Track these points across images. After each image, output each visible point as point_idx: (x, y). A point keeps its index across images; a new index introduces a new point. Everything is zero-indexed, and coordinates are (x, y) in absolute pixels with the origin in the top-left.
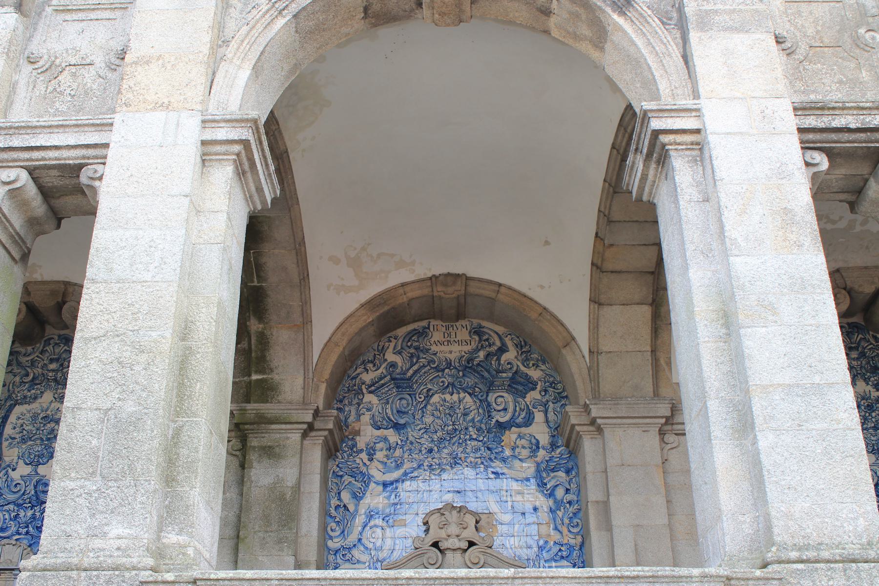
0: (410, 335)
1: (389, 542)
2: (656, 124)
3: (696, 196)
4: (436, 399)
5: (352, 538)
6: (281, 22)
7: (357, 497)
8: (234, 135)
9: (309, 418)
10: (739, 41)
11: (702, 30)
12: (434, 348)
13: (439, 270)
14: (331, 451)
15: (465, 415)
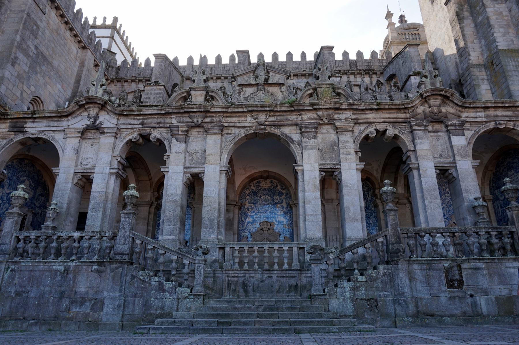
0: (256, 183)
1: (252, 228)
2: (296, 168)
3: (302, 181)
4: (262, 197)
5: (245, 227)
6: (232, 145)
7: (245, 219)
8: (225, 169)
9: (235, 203)
10: (311, 152)
11: (305, 149)
12: (262, 186)
13: (262, 170)
14: (240, 209)
15: (268, 201)
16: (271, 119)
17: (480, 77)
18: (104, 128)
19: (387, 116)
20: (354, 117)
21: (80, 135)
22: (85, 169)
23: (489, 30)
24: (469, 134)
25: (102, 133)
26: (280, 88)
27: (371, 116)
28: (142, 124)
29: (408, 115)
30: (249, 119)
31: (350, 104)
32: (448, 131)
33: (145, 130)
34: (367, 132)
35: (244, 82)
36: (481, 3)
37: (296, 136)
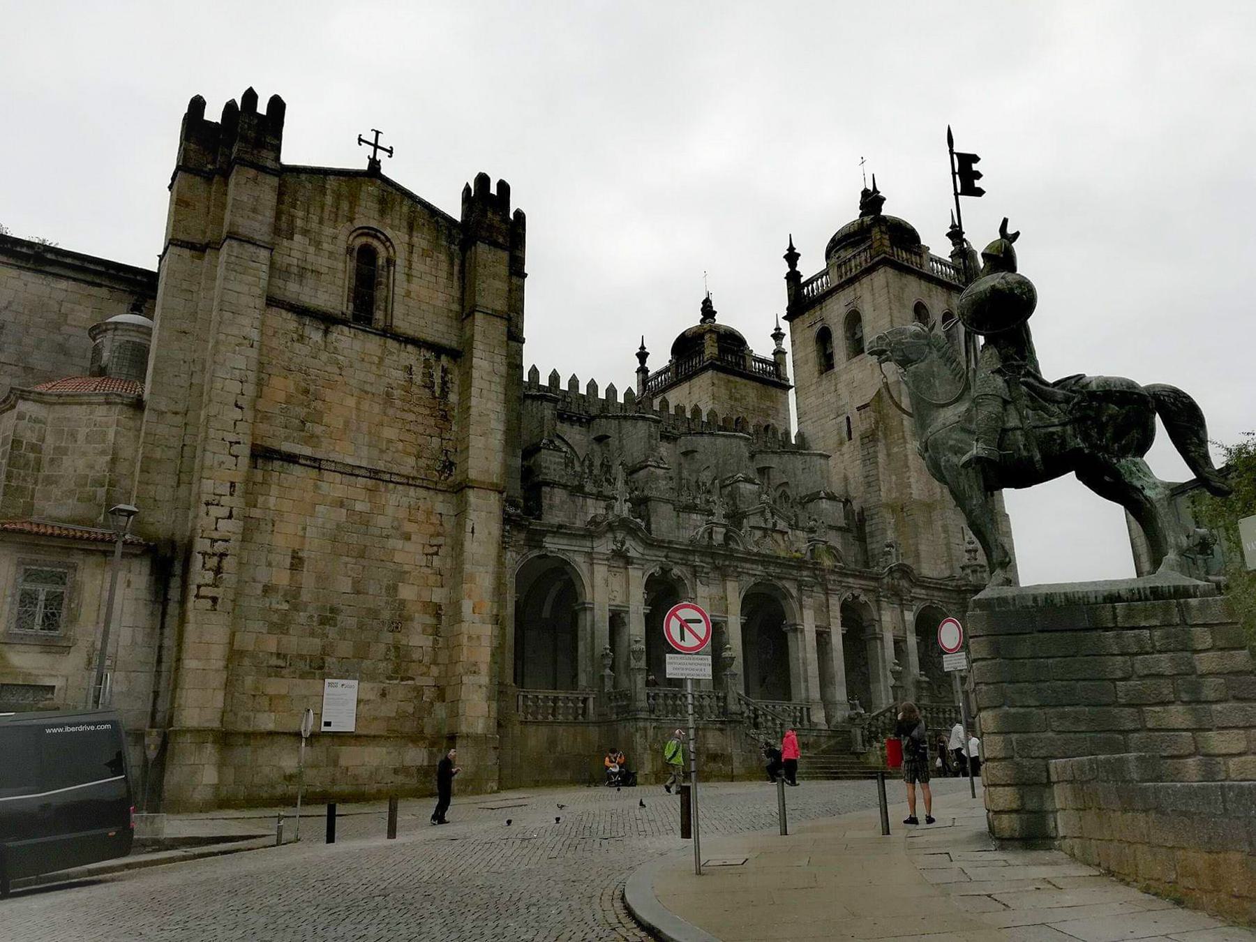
16: (778, 571)
17: (888, 521)
18: (633, 558)
19: (862, 582)
20: (840, 579)
21: (606, 562)
22: (617, 606)
23: (904, 470)
24: (914, 608)
25: (632, 563)
26: (783, 536)
27: (851, 580)
28: (666, 557)
29: (876, 585)
30: (760, 568)
31: (841, 568)
32: (901, 605)
33: (668, 565)
34: (846, 596)
35: (755, 524)
36: (901, 434)
37: (794, 592)
